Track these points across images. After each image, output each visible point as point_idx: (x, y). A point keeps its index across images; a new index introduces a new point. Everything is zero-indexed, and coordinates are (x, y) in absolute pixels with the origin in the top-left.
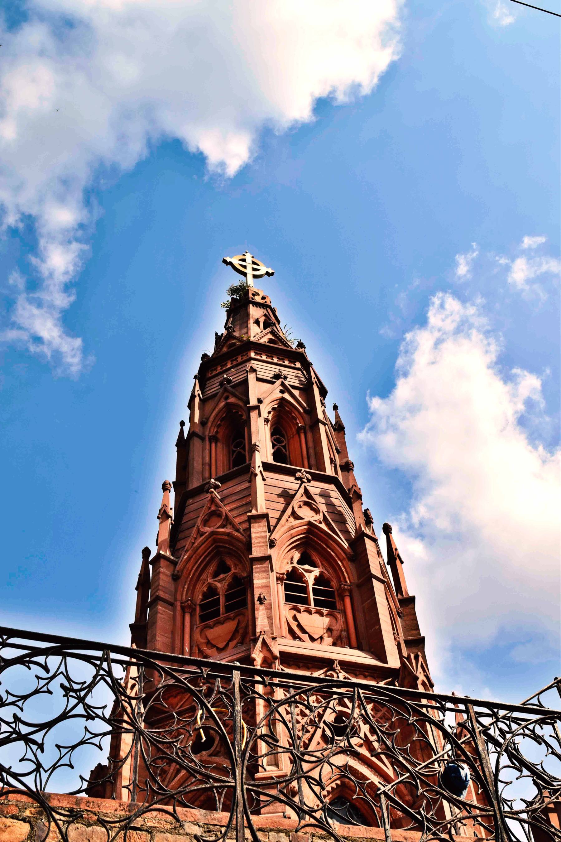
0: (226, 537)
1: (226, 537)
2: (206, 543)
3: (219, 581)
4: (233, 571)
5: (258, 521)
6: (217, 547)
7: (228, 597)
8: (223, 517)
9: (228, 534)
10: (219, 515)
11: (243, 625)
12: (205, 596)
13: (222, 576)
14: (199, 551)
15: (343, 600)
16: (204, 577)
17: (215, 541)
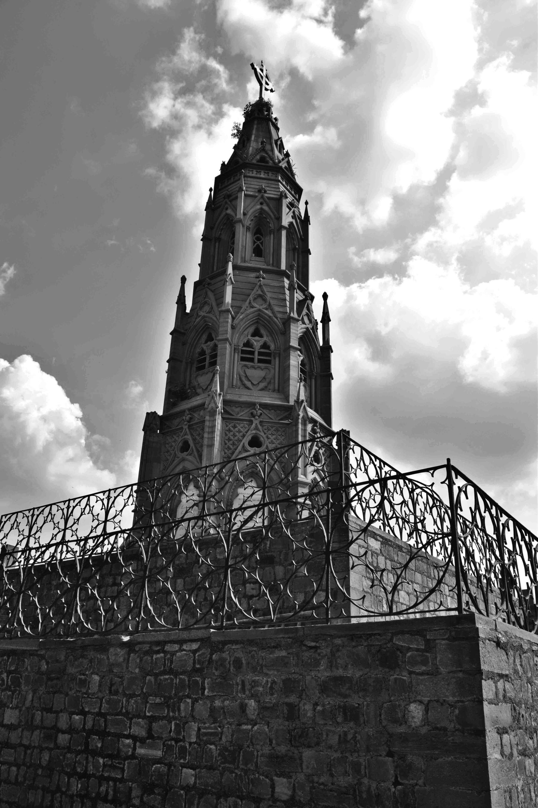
0: (268, 318)
1: (268, 318)
3: (255, 341)
4: (265, 339)
5: (295, 321)
6: (258, 318)
7: (260, 354)
8: (268, 303)
9: (270, 317)
10: (265, 300)
11: (270, 376)
12: (246, 345)
13: (257, 338)
14: (249, 317)
15: (311, 379)
16: (246, 332)
17: (259, 315)
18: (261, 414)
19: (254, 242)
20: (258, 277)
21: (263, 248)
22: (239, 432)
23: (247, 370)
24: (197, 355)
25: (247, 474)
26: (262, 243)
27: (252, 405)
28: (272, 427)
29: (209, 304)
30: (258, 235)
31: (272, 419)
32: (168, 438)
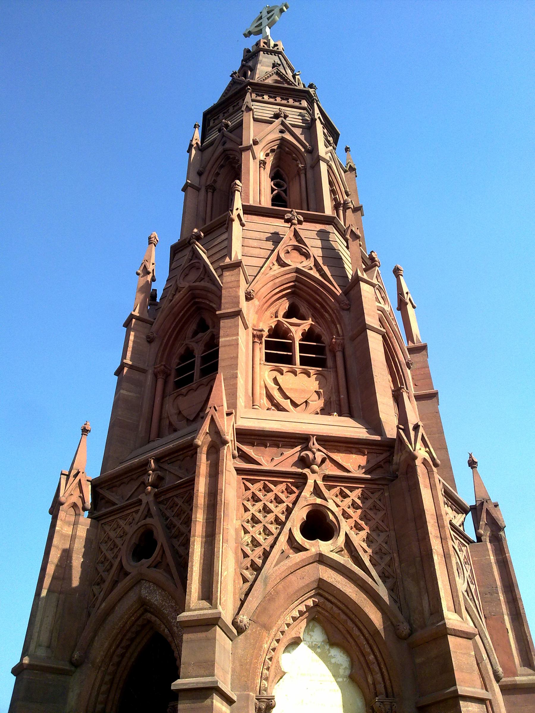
2: (287, 276)
7: (303, 348)
13: (294, 320)
18: (323, 461)
19: (273, 190)
20: (288, 221)
21: (287, 198)
22: (278, 501)
23: (280, 378)
24: (177, 361)
25: (301, 613)
26: (285, 191)
27: (302, 440)
28: (351, 489)
29: (198, 269)
30: (278, 180)
31: (348, 471)
32: (107, 528)
